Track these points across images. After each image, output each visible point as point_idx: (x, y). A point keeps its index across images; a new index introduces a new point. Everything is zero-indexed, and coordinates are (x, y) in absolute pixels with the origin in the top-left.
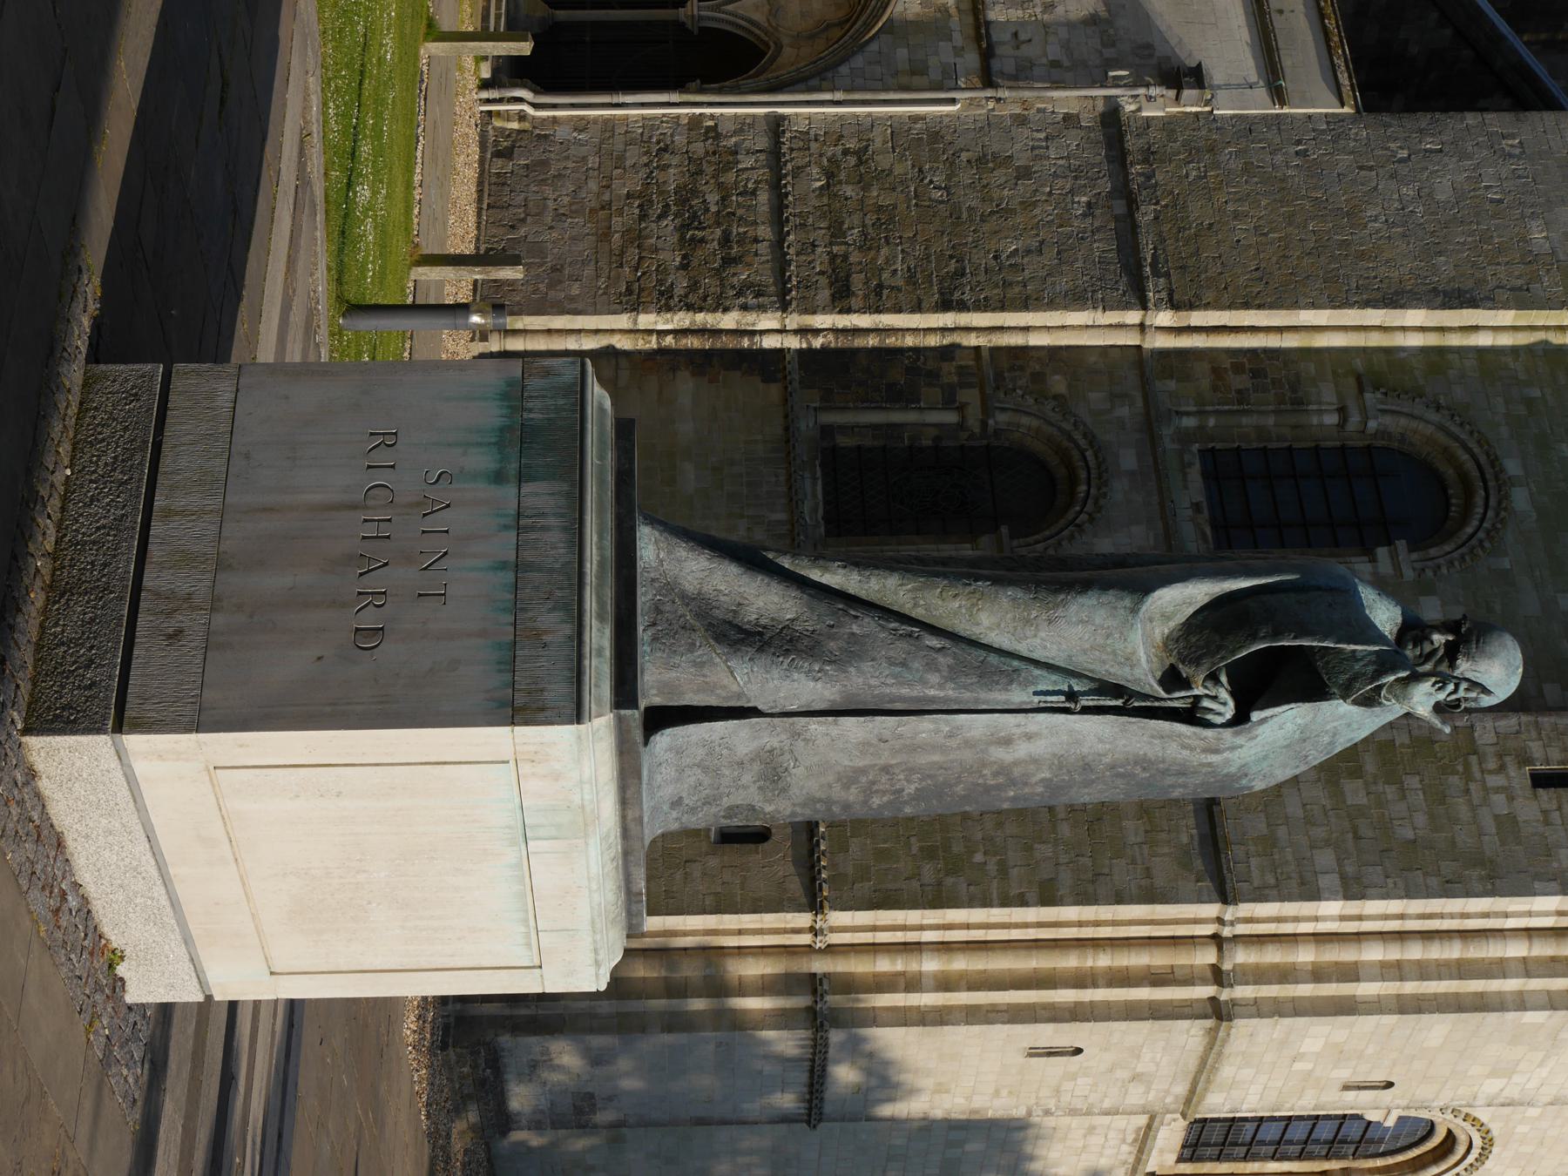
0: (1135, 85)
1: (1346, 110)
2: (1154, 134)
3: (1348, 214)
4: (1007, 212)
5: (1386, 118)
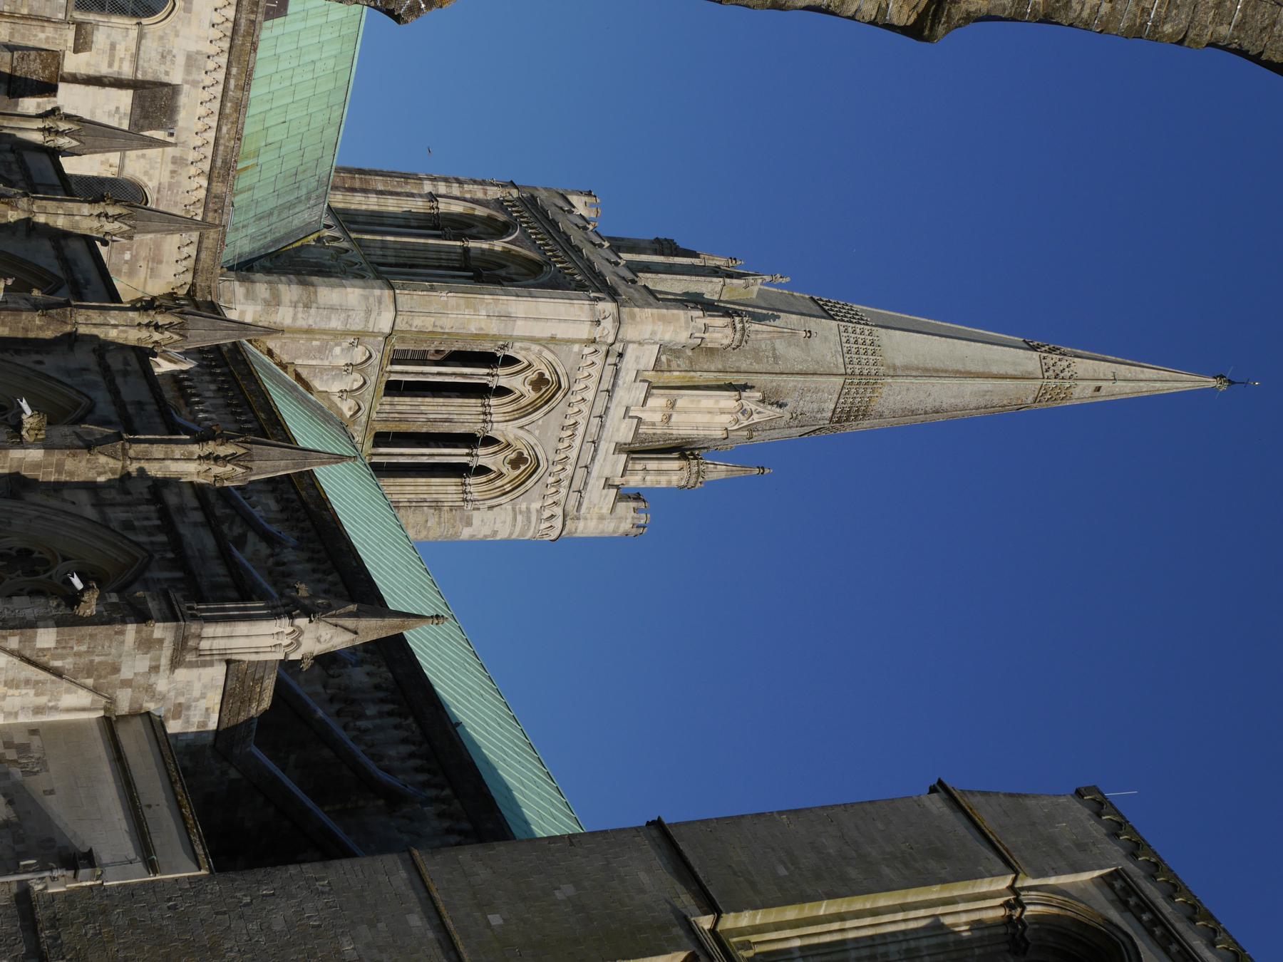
0: (41, 870)
1: (203, 872)
2: (58, 905)
3: (210, 949)
5: (232, 875)
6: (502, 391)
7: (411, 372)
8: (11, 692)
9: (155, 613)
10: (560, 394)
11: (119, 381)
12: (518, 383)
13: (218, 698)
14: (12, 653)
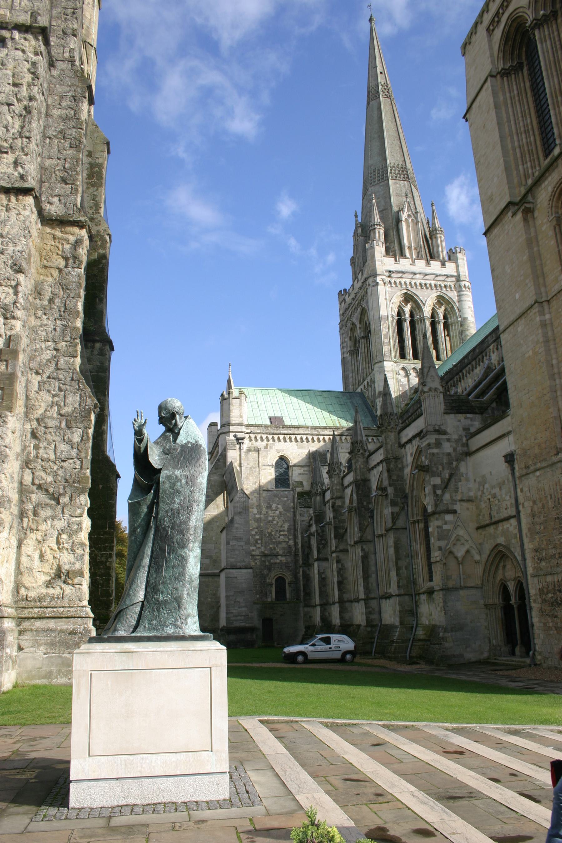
4: (543, 506)
6: (412, 315)
7: (409, 351)
8: (460, 491)
9: (426, 443)
10: (409, 292)
11: (375, 463)
12: (407, 309)
13: (460, 415)
14: (443, 492)
